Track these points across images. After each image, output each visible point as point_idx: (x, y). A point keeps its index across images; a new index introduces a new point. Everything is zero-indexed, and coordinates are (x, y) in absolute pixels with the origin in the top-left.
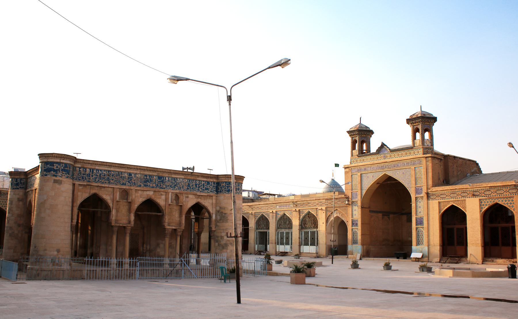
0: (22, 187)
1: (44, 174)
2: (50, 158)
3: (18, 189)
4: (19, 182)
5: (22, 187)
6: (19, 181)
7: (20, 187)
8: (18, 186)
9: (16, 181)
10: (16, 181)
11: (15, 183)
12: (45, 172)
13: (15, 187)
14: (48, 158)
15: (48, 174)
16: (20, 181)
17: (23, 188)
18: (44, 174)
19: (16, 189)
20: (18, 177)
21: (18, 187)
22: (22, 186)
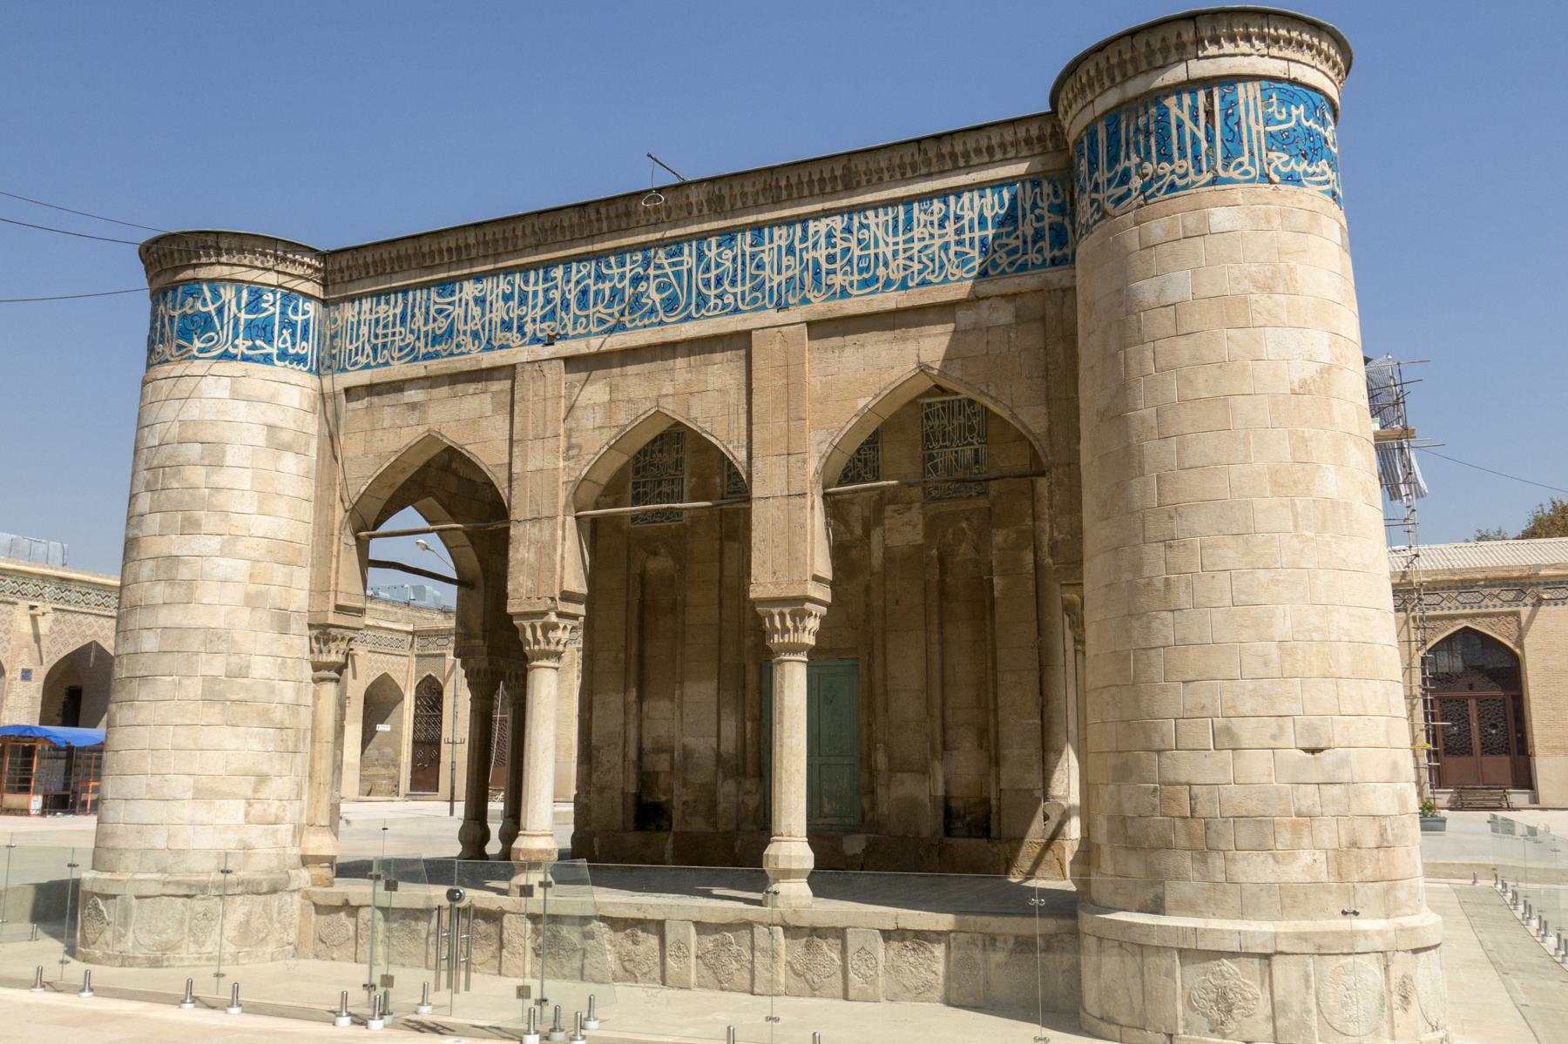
0: (291, 351)
1: (1277, 171)
2: (1306, 57)
3: (267, 359)
4: (274, 314)
5: (291, 351)
6: (272, 305)
7: (283, 355)
8: (270, 342)
9: (254, 305)
10: (254, 305)
11: (243, 316)
12: (1286, 157)
13: (242, 345)
14: (1288, 53)
15: (1306, 173)
16: (282, 313)
17: (300, 359)
18: (1277, 171)
19: (245, 359)
20: (272, 278)
21: (268, 350)
22: (294, 345)
